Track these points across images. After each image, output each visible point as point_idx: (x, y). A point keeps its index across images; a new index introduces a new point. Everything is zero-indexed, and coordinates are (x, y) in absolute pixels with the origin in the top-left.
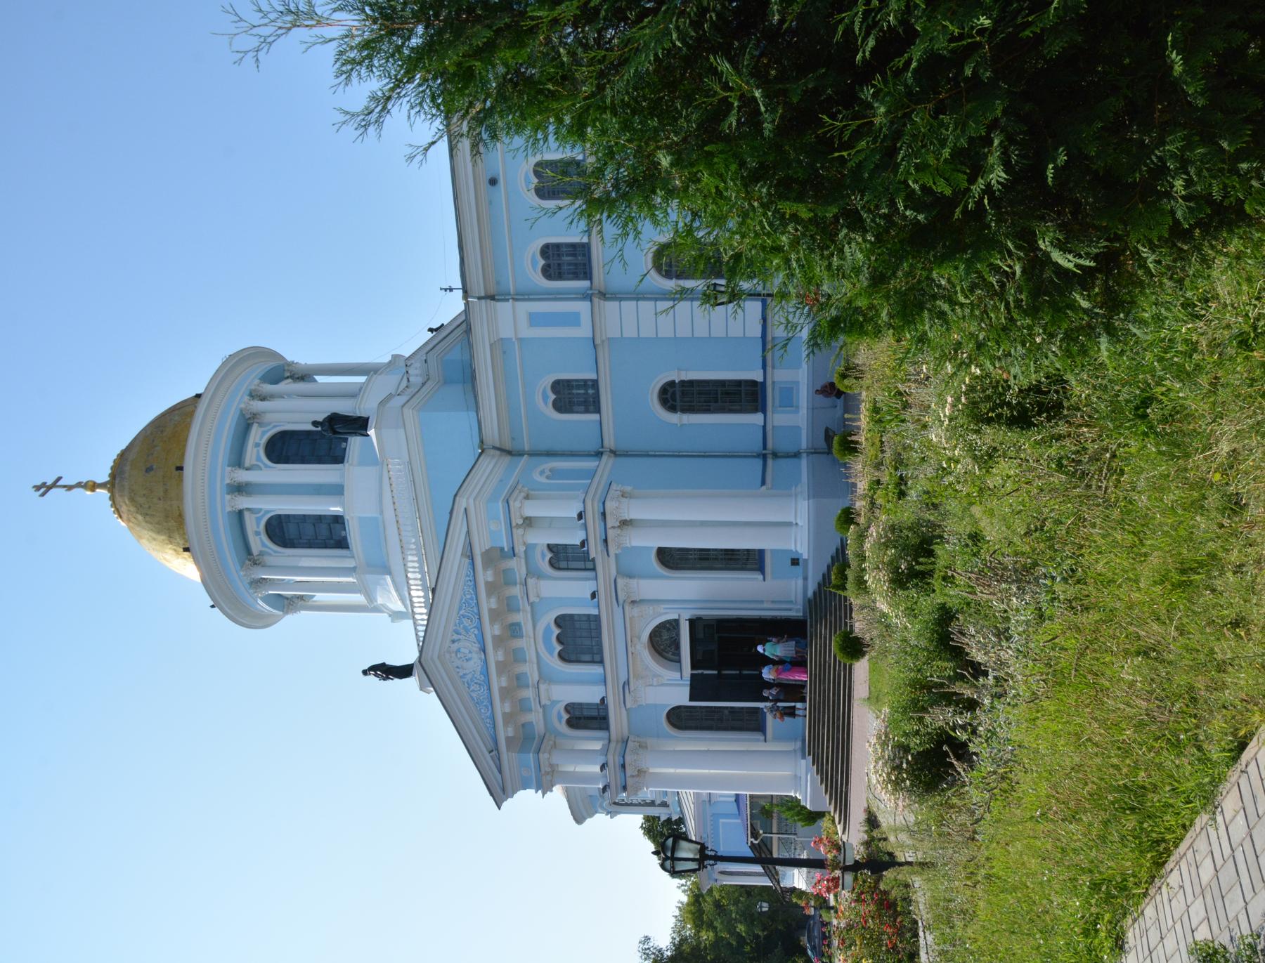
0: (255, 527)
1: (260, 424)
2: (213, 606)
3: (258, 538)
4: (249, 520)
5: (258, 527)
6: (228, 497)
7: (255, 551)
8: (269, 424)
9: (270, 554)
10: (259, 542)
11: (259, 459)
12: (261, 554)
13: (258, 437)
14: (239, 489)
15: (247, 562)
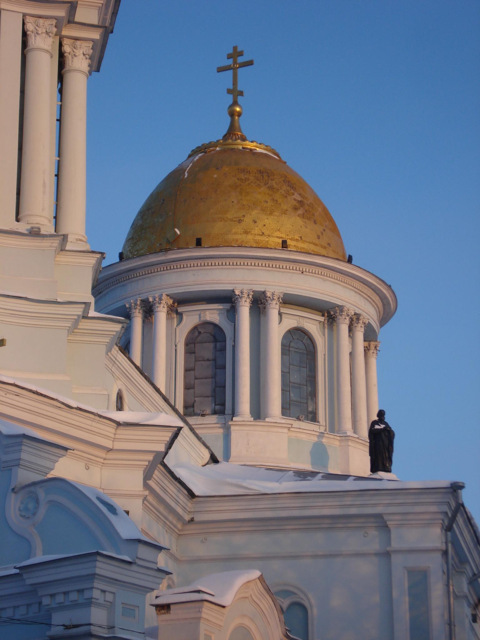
7: (180, 310)
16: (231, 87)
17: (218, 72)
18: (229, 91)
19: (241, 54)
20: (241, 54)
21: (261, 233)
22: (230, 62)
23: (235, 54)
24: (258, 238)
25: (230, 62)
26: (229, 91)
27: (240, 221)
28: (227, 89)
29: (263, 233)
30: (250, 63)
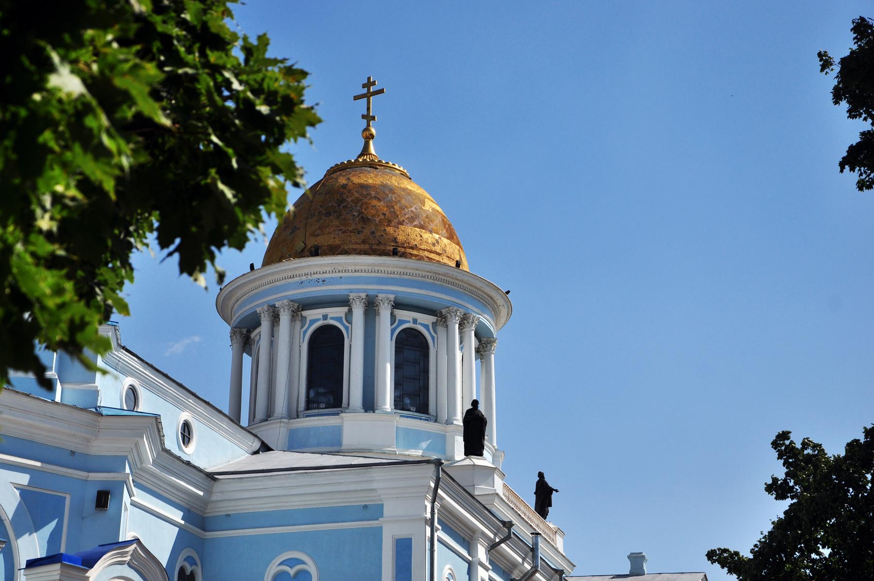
0: (334, 314)
1: (434, 324)
2: (252, 267)
3: (321, 317)
4: (341, 311)
5: (331, 318)
6: (363, 295)
7: (305, 313)
8: (436, 333)
9: (302, 327)
10: (316, 317)
11: (402, 322)
12: (303, 319)
13: (423, 321)
14: (371, 307)
15: (296, 305)
16: (365, 113)
17: (354, 100)
18: (363, 117)
19: (374, 83)
20: (374, 83)
21: (378, 243)
22: (365, 91)
23: (369, 84)
24: (375, 247)
25: (365, 91)
26: (363, 117)
27: (359, 233)
28: (362, 115)
29: (380, 243)
30: (381, 91)
